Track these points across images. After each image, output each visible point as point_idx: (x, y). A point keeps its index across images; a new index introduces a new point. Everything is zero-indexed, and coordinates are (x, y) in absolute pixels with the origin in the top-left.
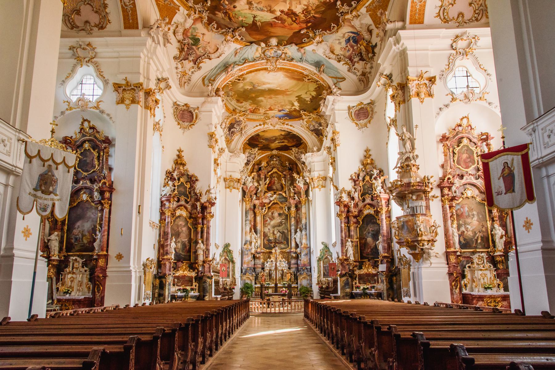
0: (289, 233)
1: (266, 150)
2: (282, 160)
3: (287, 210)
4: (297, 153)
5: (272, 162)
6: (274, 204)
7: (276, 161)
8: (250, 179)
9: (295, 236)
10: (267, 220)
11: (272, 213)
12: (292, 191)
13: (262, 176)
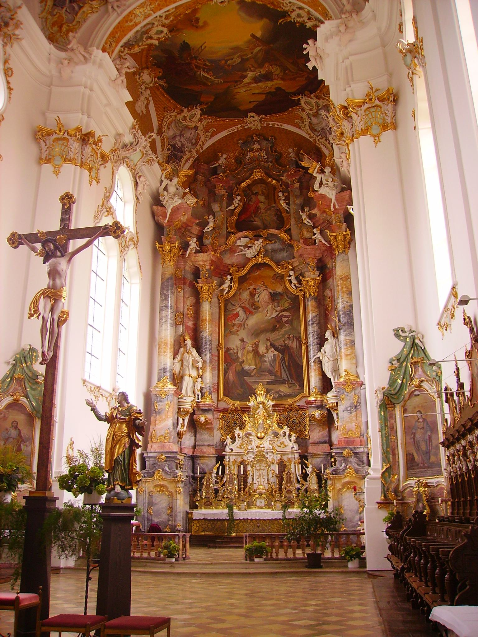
0: (304, 348)
1: (227, 118)
2: (279, 149)
3: (294, 282)
4: (314, 116)
5: (250, 155)
6: (258, 266)
7: (260, 150)
8: (173, 185)
9: (319, 355)
10: (237, 315)
11: (252, 295)
12: (307, 221)
13: (221, 192)
